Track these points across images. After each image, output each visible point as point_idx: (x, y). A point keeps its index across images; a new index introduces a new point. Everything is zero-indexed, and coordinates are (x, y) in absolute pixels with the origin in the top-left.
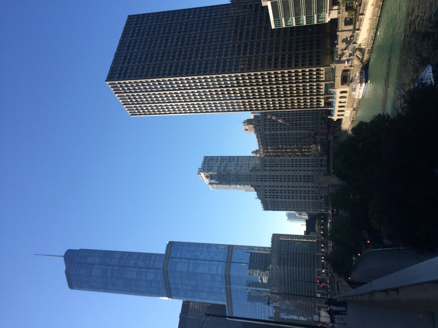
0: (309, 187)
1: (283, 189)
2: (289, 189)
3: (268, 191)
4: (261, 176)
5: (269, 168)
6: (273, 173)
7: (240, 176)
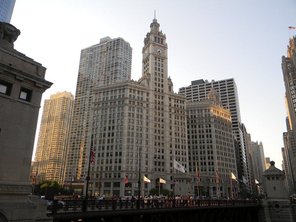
0: (147, 164)
1: (145, 121)
2: (144, 131)
3: (140, 96)
4: (163, 90)
5: (173, 105)
6: (167, 109)
7: (162, 62)
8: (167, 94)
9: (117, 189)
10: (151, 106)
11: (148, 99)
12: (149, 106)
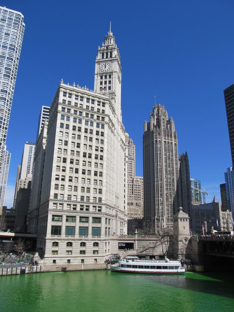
9: (98, 225)
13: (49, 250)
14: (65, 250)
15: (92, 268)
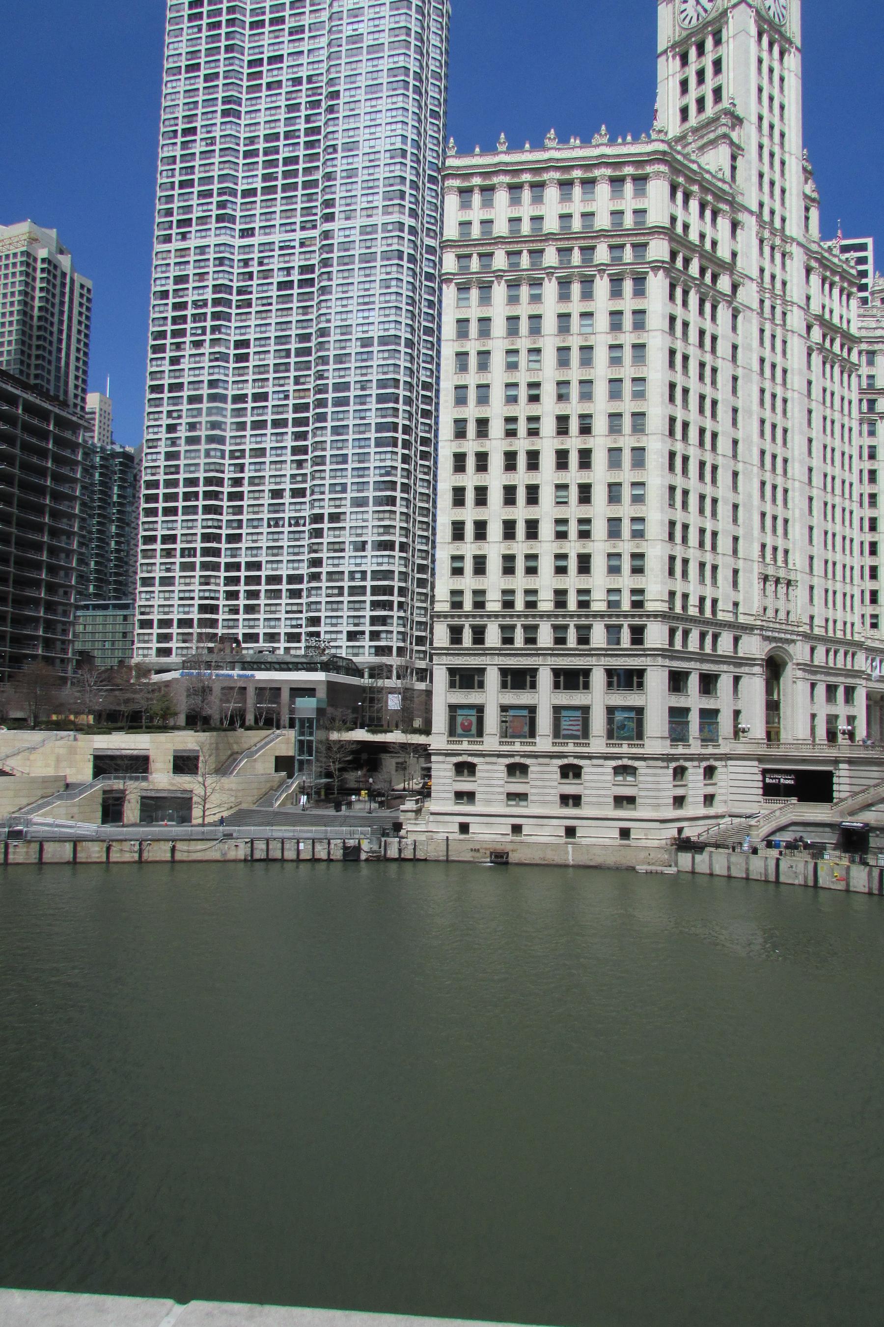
6: (796, 320)
8: (802, 246)
9: (632, 699)
10: (748, 294)
11: (734, 255)
12: (741, 291)
13: (442, 788)
14: (501, 790)
15: (610, 859)
